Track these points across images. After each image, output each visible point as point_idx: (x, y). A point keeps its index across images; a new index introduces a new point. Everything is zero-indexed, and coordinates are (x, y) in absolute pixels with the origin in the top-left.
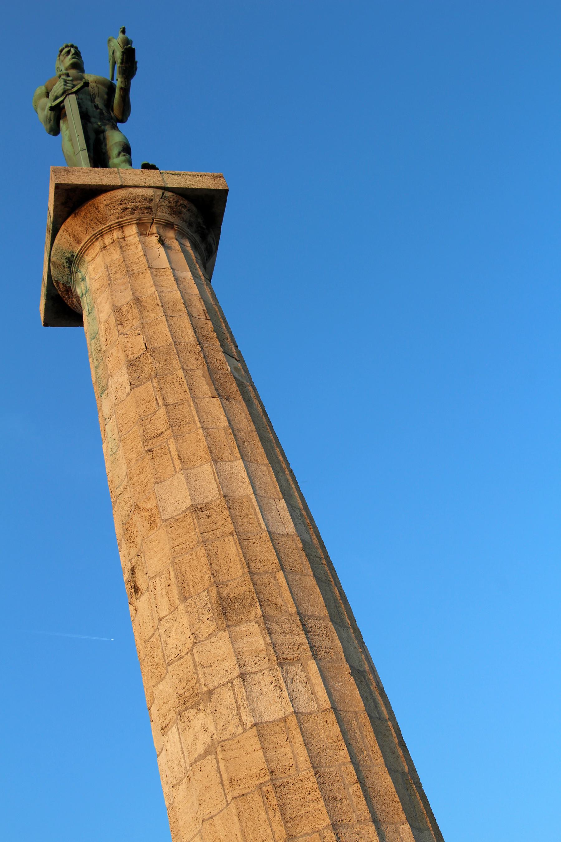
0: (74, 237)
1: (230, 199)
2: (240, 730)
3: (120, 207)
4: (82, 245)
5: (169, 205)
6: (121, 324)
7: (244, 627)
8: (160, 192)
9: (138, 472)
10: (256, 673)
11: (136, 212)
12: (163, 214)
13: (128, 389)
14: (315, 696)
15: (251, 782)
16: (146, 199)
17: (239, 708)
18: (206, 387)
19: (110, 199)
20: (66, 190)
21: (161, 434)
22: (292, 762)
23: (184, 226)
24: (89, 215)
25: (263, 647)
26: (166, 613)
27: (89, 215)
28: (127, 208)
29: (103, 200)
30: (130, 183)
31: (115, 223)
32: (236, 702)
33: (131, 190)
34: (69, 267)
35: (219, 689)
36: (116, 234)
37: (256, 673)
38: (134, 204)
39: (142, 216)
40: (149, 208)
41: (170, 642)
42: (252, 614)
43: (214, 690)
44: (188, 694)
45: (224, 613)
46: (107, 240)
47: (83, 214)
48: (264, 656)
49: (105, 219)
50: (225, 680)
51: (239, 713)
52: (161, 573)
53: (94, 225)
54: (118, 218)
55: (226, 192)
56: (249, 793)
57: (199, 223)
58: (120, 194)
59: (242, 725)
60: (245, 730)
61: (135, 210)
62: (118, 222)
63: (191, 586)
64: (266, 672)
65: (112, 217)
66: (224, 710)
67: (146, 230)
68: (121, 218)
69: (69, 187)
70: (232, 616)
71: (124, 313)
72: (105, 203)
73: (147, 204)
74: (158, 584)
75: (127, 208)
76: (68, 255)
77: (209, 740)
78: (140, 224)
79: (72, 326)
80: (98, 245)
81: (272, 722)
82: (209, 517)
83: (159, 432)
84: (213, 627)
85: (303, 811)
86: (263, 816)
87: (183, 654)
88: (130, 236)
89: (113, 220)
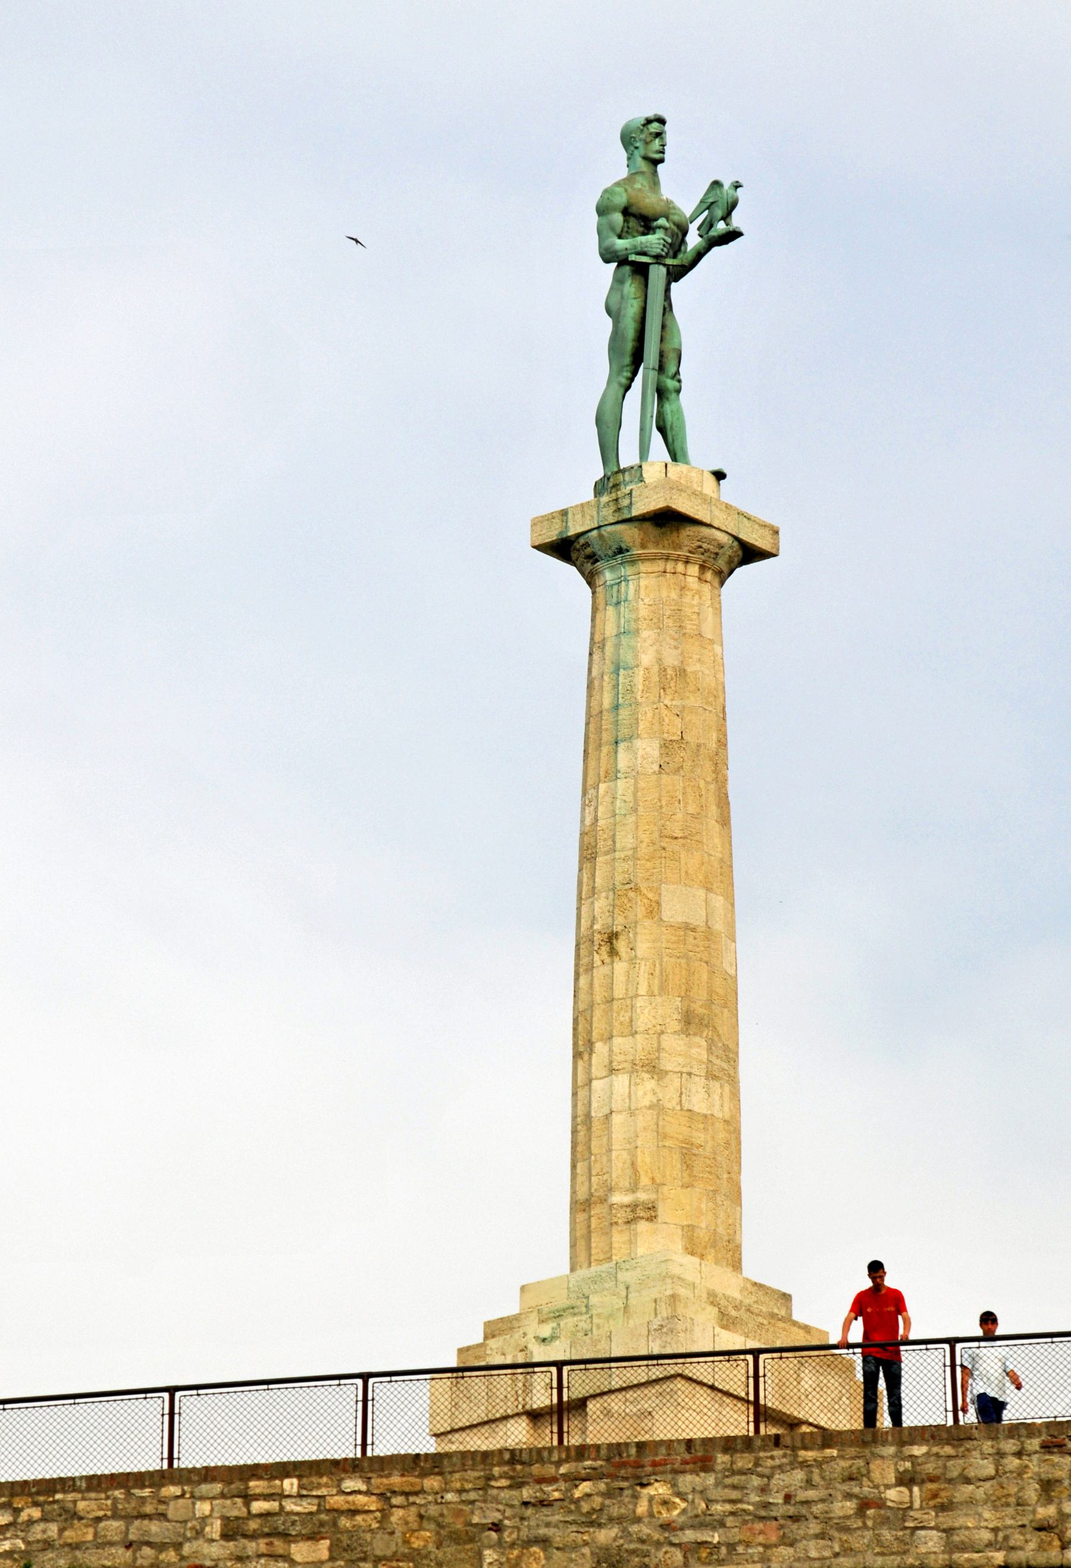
2: (678, 1108)
4: (646, 551)
6: (664, 689)
7: (697, 1039)
9: (647, 857)
10: (697, 1075)
11: (706, 554)
13: (656, 768)
15: (677, 1143)
16: (719, 544)
17: (681, 1093)
18: (714, 807)
21: (676, 838)
22: (703, 1144)
25: (705, 1061)
28: (700, 547)
29: (689, 531)
30: (716, 524)
36: (680, 567)
37: (697, 1075)
38: (709, 546)
40: (717, 554)
41: (642, 1016)
42: (705, 1034)
44: (646, 1062)
45: (688, 1022)
46: (670, 566)
47: (664, 529)
49: (678, 547)
50: (677, 1069)
51: (680, 1097)
52: (647, 959)
53: (667, 545)
54: (690, 552)
58: (705, 531)
59: (681, 1105)
60: (682, 1110)
64: (703, 1078)
65: (687, 548)
66: (672, 1089)
70: (693, 1028)
71: (668, 676)
72: (688, 533)
73: (717, 550)
74: (643, 967)
75: (700, 547)
76: (624, 546)
77: (655, 1101)
78: (703, 568)
80: (660, 565)
82: (695, 939)
83: (675, 835)
84: (678, 1028)
85: (701, 1175)
86: (679, 1166)
87: (650, 1032)
89: (684, 553)
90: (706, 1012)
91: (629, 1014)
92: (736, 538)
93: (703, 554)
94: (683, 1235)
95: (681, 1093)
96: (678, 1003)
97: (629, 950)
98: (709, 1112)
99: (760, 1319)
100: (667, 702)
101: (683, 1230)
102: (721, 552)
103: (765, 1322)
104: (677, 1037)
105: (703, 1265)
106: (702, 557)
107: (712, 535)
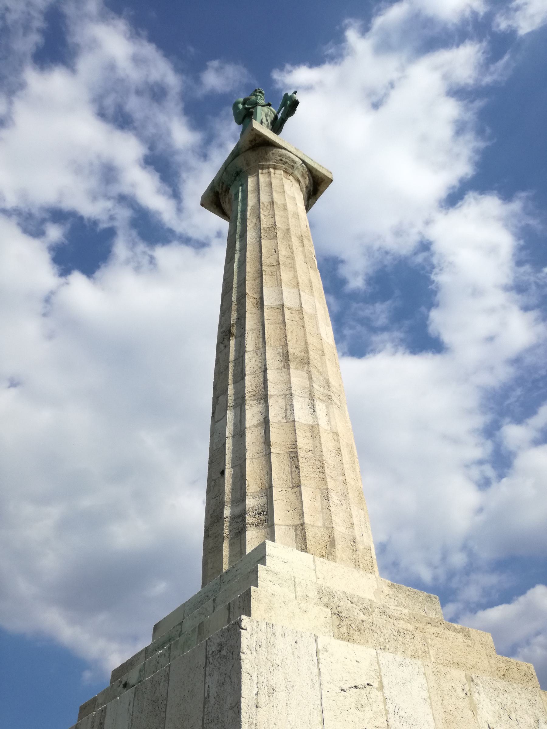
0: (247, 161)
1: (331, 185)
2: (284, 421)
3: (279, 158)
5: (303, 171)
8: (301, 162)
11: (286, 165)
12: (298, 174)
14: (330, 423)
19: (275, 151)
20: (256, 134)
21: (273, 266)
23: (304, 187)
24: (261, 153)
26: (251, 350)
27: (261, 153)
28: (281, 160)
31: (272, 164)
32: (286, 406)
33: (288, 153)
34: (235, 177)
35: (276, 396)
38: (287, 160)
39: (287, 168)
43: (273, 395)
47: (257, 152)
48: (308, 391)
54: (275, 162)
55: (332, 181)
56: (282, 454)
57: (310, 190)
58: (283, 151)
61: (285, 163)
62: (274, 165)
63: (272, 341)
67: (287, 176)
68: (276, 163)
69: (258, 133)
71: (265, 205)
76: (238, 170)
79: (214, 213)
81: (305, 424)
88: (278, 174)
90: (306, 355)
91: (241, 367)
92: (304, 162)
93: (284, 164)
94: (296, 535)
95: (286, 410)
96: (279, 350)
97: (241, 329)
98: (315, 423)
99: (402, 625)
100: (265, 213)
101: (296, 530)
102: (295, 165)
103: (411, 628)
104: (280, 371)
105: (318, 563)
106: (284, 166)
107: (287, 154)
